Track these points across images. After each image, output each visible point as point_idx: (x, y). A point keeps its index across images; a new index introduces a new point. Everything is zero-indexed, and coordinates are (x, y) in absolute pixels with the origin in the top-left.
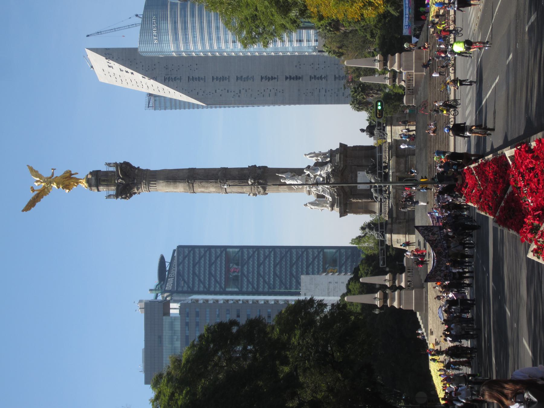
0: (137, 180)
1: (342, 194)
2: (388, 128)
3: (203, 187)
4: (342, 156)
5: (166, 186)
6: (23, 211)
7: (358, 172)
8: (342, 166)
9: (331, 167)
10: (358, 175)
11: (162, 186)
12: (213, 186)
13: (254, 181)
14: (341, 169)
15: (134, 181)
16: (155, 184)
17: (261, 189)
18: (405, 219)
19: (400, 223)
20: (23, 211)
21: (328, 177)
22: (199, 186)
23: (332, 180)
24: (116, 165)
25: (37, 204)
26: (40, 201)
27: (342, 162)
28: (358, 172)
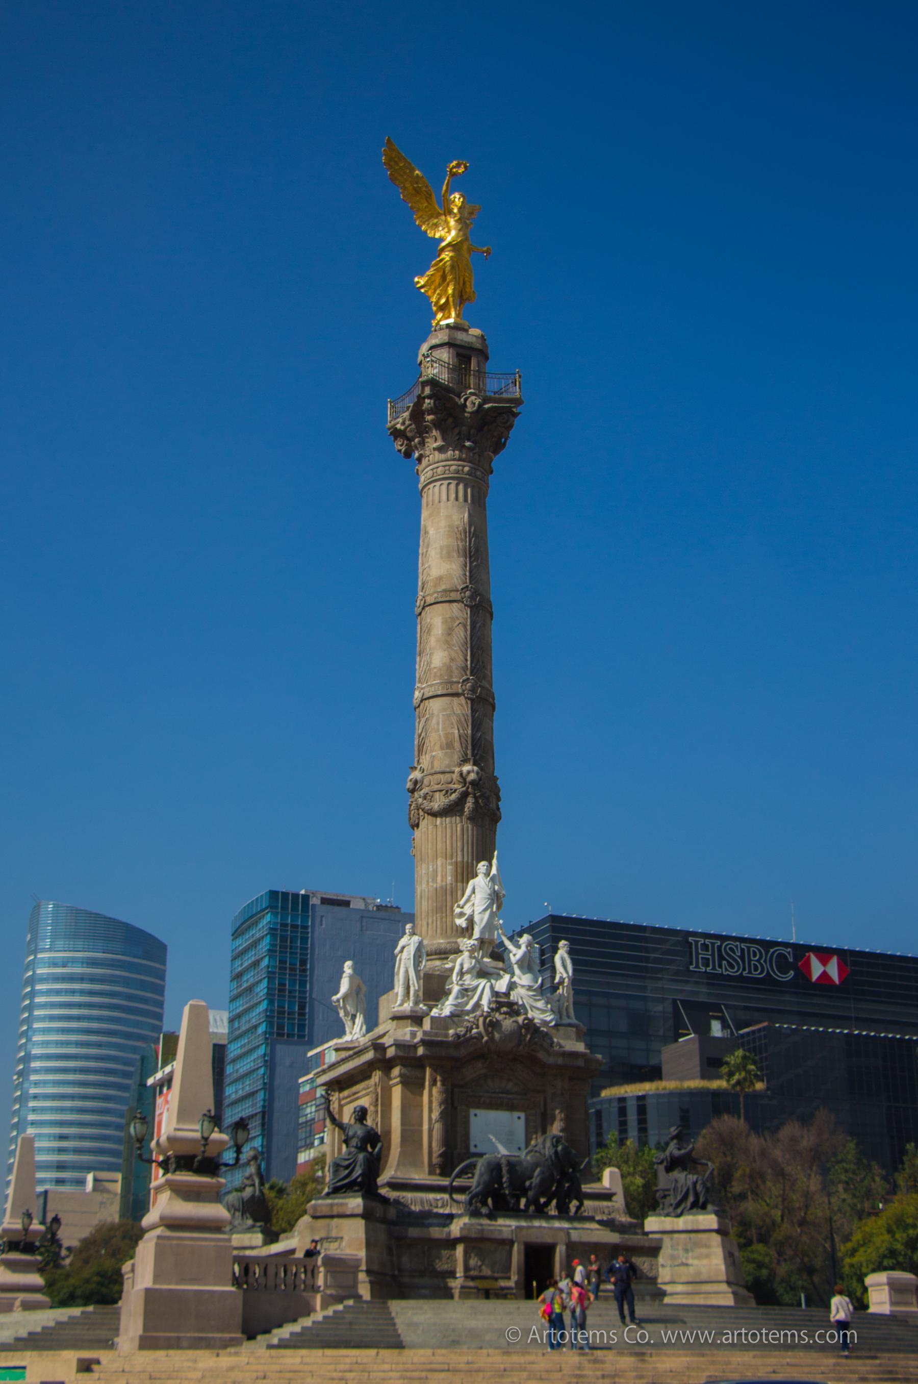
0: (469, 448)
1: (463, 1052)
2: (709, 1220)
3: (449, 631)
4: (581, 1063)
5: (451, 527)
7: (522, 1115)
8: (551, 1060)
9: (546, 1023)
10: (516, 1114)
11: (449, 517)
12: (452, 660)
13: (473, 783)
14: (541, 1055)
15: (469, 440)
16: (457, 499)
17: (439, 802)
18: (400, 1270)
19: (390, 1249)
21: (514, 1009)
22: (453, 619)
23: (508, 1024)
27: (560, 1061)
28: (522, 1115)
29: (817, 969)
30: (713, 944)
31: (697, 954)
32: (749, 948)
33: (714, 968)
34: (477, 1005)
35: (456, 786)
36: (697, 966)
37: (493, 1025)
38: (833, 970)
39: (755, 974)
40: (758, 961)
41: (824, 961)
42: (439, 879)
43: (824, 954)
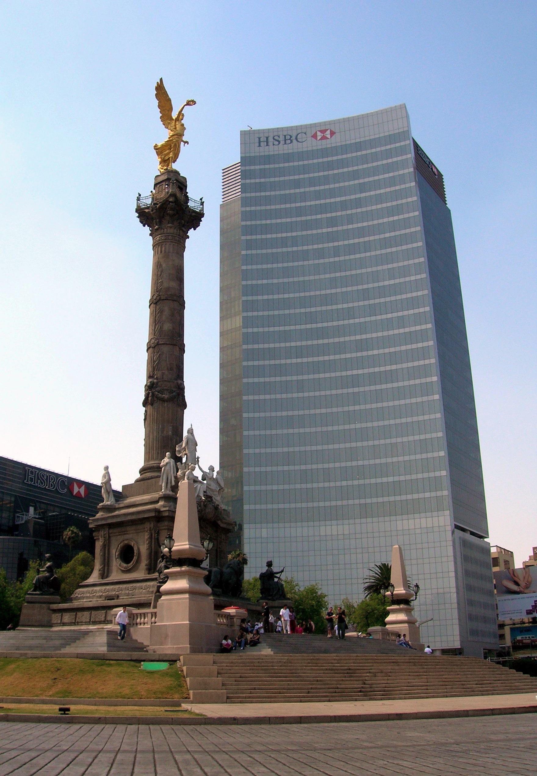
6: (161, 80)
8: (222, 525)
14: (219, 522)
20: (161, 80)
24: (202, 215)
25: (156, 102)
26: (159, 107)
29: (76, 490)
30: (35, 472)
31: (28, 475)
32: (50, 476)
33: (34, 483)
34: (198, 496)
35: (174, 389)
36: (27, 481)
37: (205, 506)
38: (82, 490)
39: (51, 488)
40: (53, 482)
41: (80, 487)
42: (165, 432)
43: (81, 483)
